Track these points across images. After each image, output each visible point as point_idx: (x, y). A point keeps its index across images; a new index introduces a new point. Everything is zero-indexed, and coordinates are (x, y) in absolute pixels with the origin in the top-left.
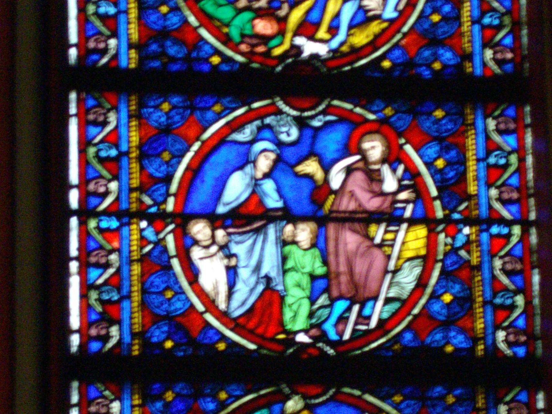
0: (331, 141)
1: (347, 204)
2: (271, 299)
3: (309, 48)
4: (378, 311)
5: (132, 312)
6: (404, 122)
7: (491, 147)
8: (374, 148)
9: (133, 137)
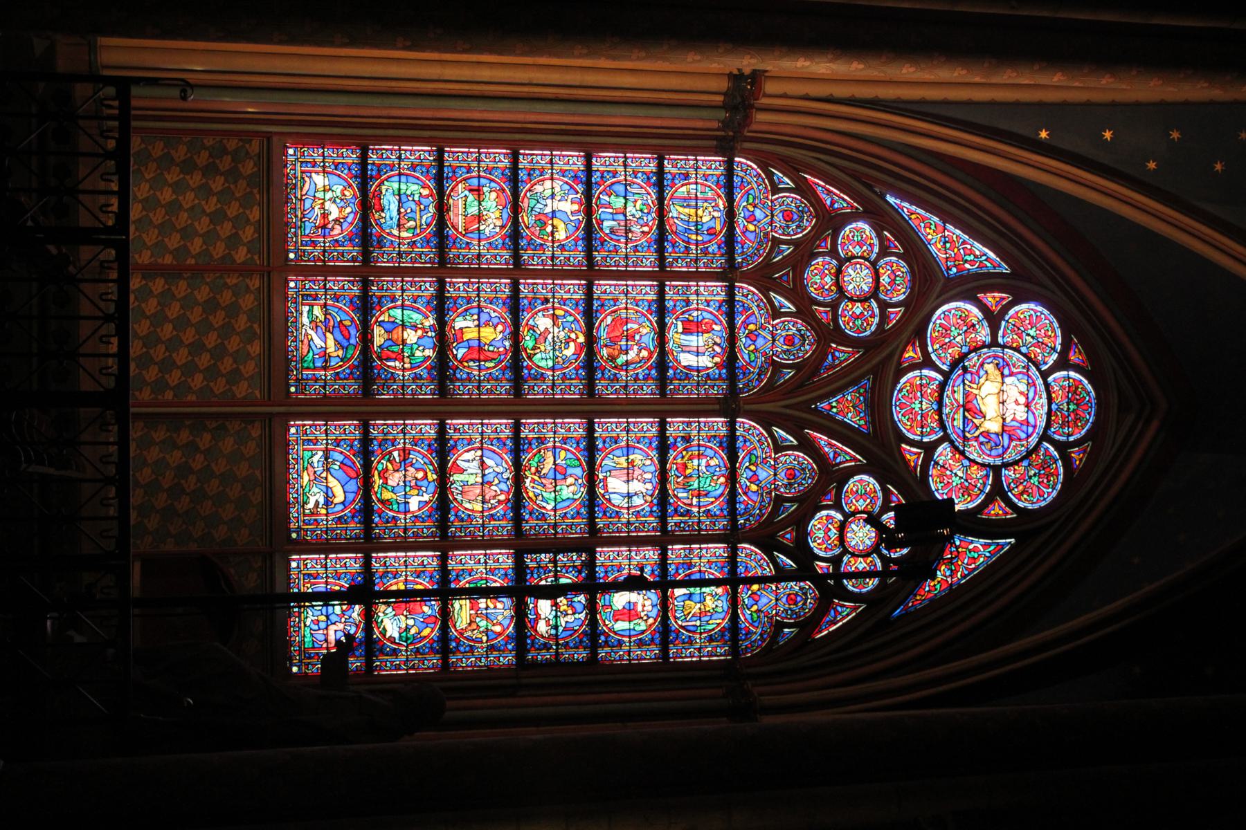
0: (504, 487)
1: (487, 490)
2: (462, 471)
3: (528, 481)
4: (459, 498)
5: (457, 436)
6: (509, 505)
7: (503, 528)
8: (502, 497)
9: (502, 436)
